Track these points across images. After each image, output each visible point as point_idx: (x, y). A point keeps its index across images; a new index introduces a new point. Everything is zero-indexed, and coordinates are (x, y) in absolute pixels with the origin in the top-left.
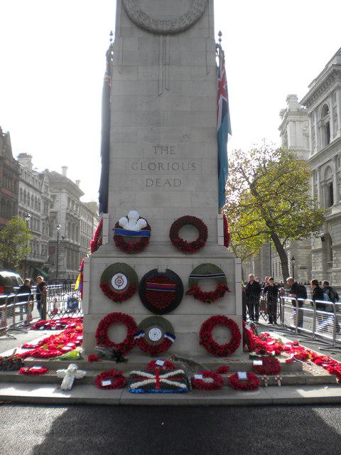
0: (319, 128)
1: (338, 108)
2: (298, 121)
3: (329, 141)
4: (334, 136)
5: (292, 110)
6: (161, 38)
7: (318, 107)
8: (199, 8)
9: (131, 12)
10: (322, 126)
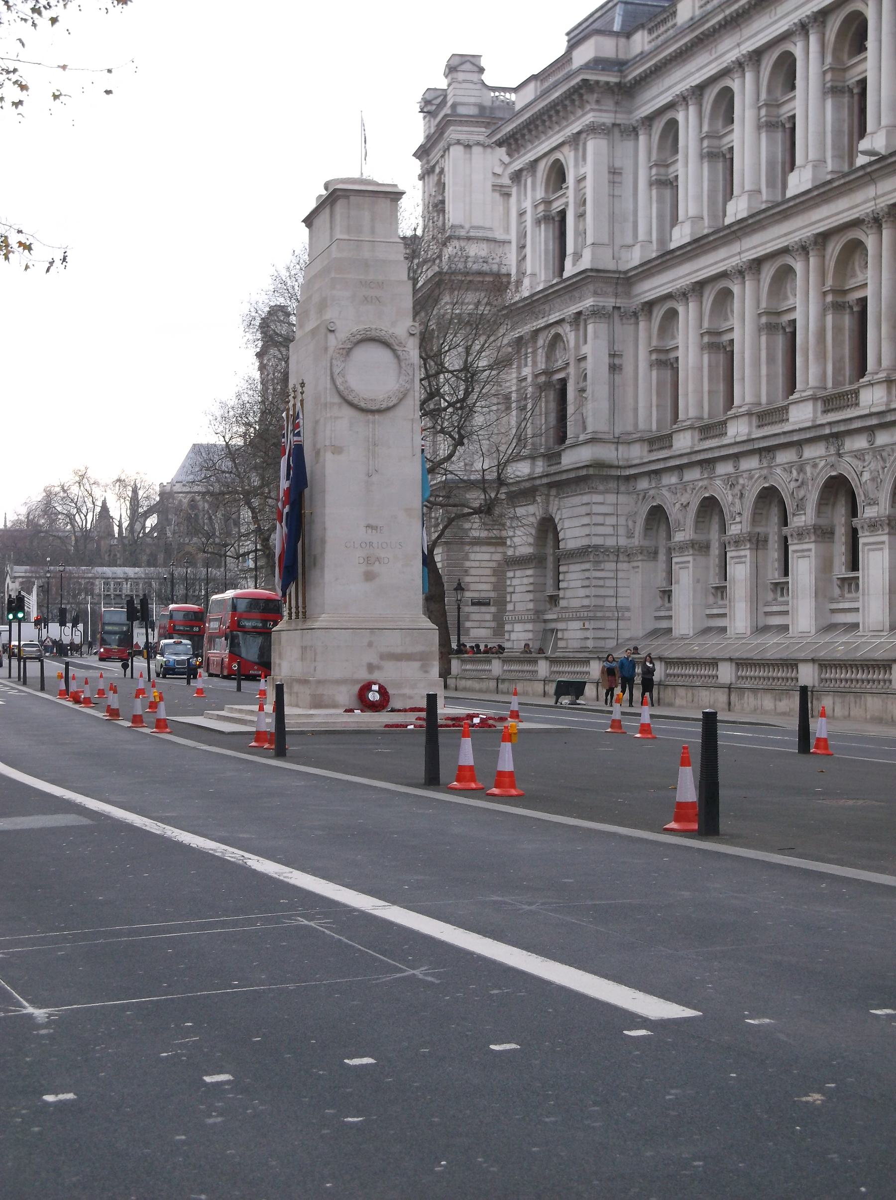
0: (538, 222)
1: (589, 183)
2: (478, 144)
3: (562, 269)
4: (578, 256)
5: (461, 110)
6: (370, 417)
7: (536, 161)
8: (407, 385)
9: (341, 388)
10: (547, 218)
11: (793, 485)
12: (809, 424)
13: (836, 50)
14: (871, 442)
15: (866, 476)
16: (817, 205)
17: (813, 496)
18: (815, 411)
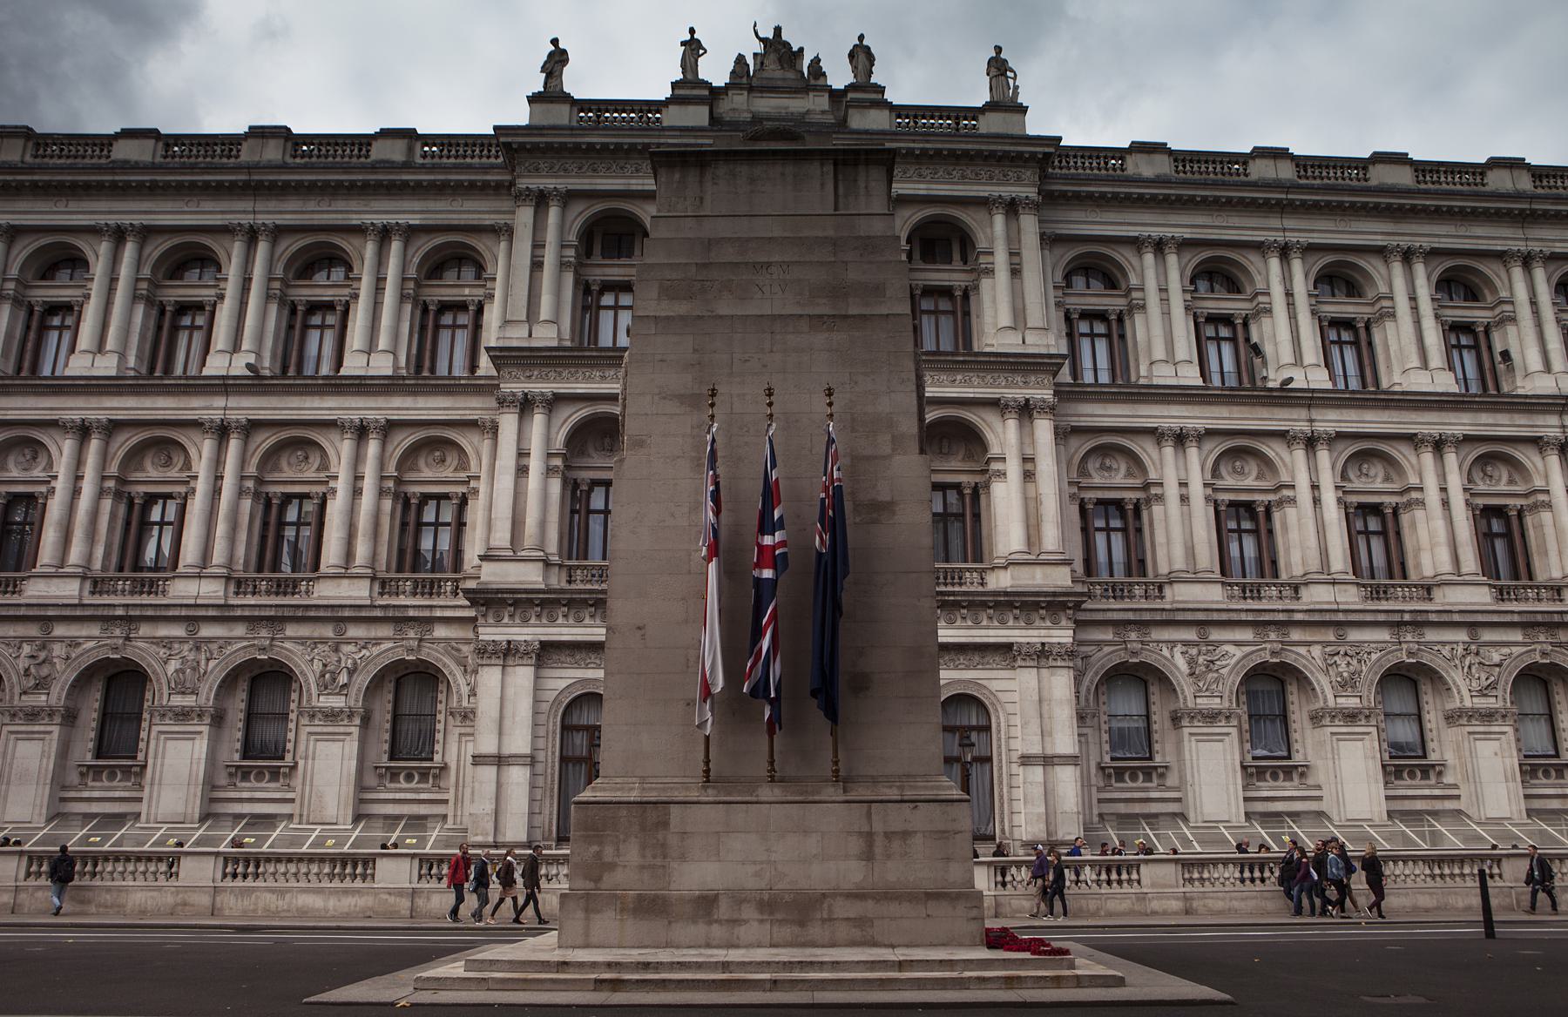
11: (23, 663)
12: (76, 601)
13: (155, 268)
14: (192, 633)
15: (173, 666)
16: (120, 394)
17: (65, 676)
18: (81, 590)
